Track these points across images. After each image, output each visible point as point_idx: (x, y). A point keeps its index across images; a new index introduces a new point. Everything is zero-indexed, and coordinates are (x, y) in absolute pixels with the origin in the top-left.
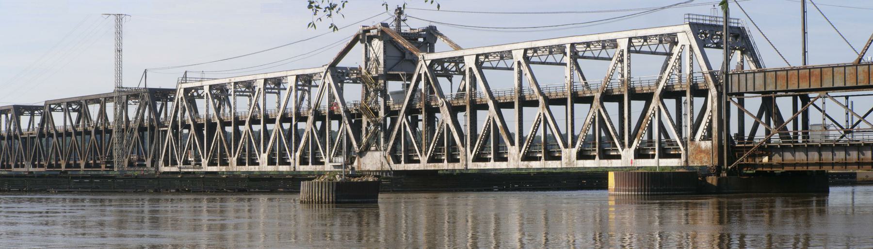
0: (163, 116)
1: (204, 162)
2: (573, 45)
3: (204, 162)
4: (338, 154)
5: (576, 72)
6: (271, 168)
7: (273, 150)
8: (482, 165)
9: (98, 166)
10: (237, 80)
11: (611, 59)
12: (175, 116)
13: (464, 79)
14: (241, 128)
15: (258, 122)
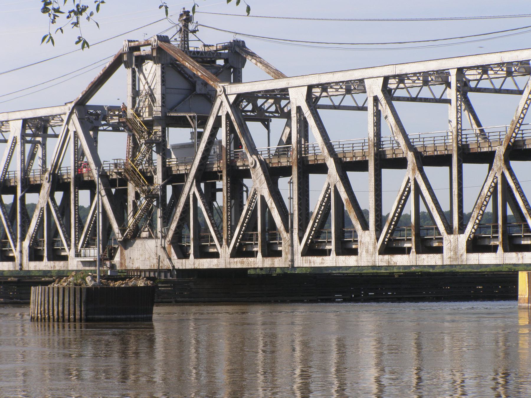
2: (460, 71)
4: (88, 244)
5: (466, 114)
8: (317, 261)
11: (521, 92)
13: (288, 124)
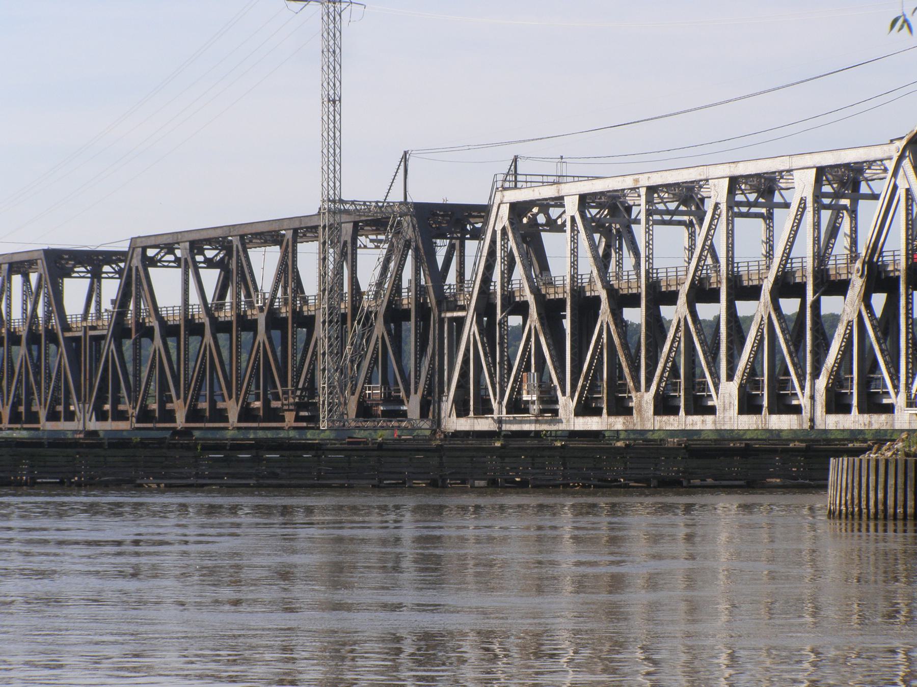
0: (452, 278)
1: (566, 404)
3: (566, 404)
6: (748, 422)
7: (753, 372)
9: (275, 415)
10: (657, 179)
12: (487, 280)
14: (667, 312)
15: (712, 296)
